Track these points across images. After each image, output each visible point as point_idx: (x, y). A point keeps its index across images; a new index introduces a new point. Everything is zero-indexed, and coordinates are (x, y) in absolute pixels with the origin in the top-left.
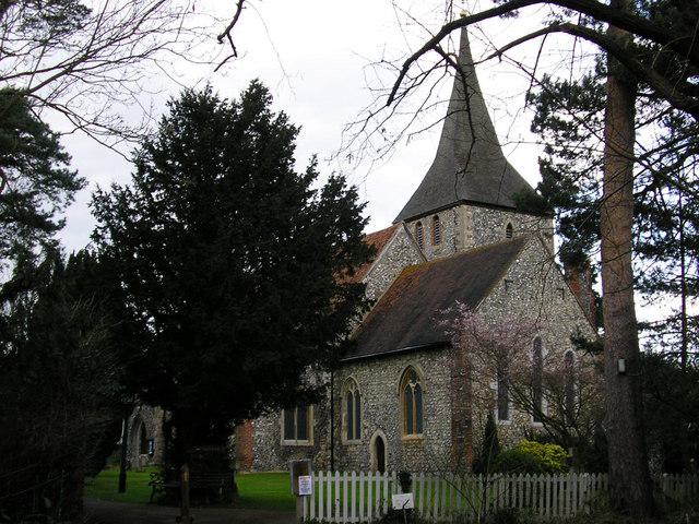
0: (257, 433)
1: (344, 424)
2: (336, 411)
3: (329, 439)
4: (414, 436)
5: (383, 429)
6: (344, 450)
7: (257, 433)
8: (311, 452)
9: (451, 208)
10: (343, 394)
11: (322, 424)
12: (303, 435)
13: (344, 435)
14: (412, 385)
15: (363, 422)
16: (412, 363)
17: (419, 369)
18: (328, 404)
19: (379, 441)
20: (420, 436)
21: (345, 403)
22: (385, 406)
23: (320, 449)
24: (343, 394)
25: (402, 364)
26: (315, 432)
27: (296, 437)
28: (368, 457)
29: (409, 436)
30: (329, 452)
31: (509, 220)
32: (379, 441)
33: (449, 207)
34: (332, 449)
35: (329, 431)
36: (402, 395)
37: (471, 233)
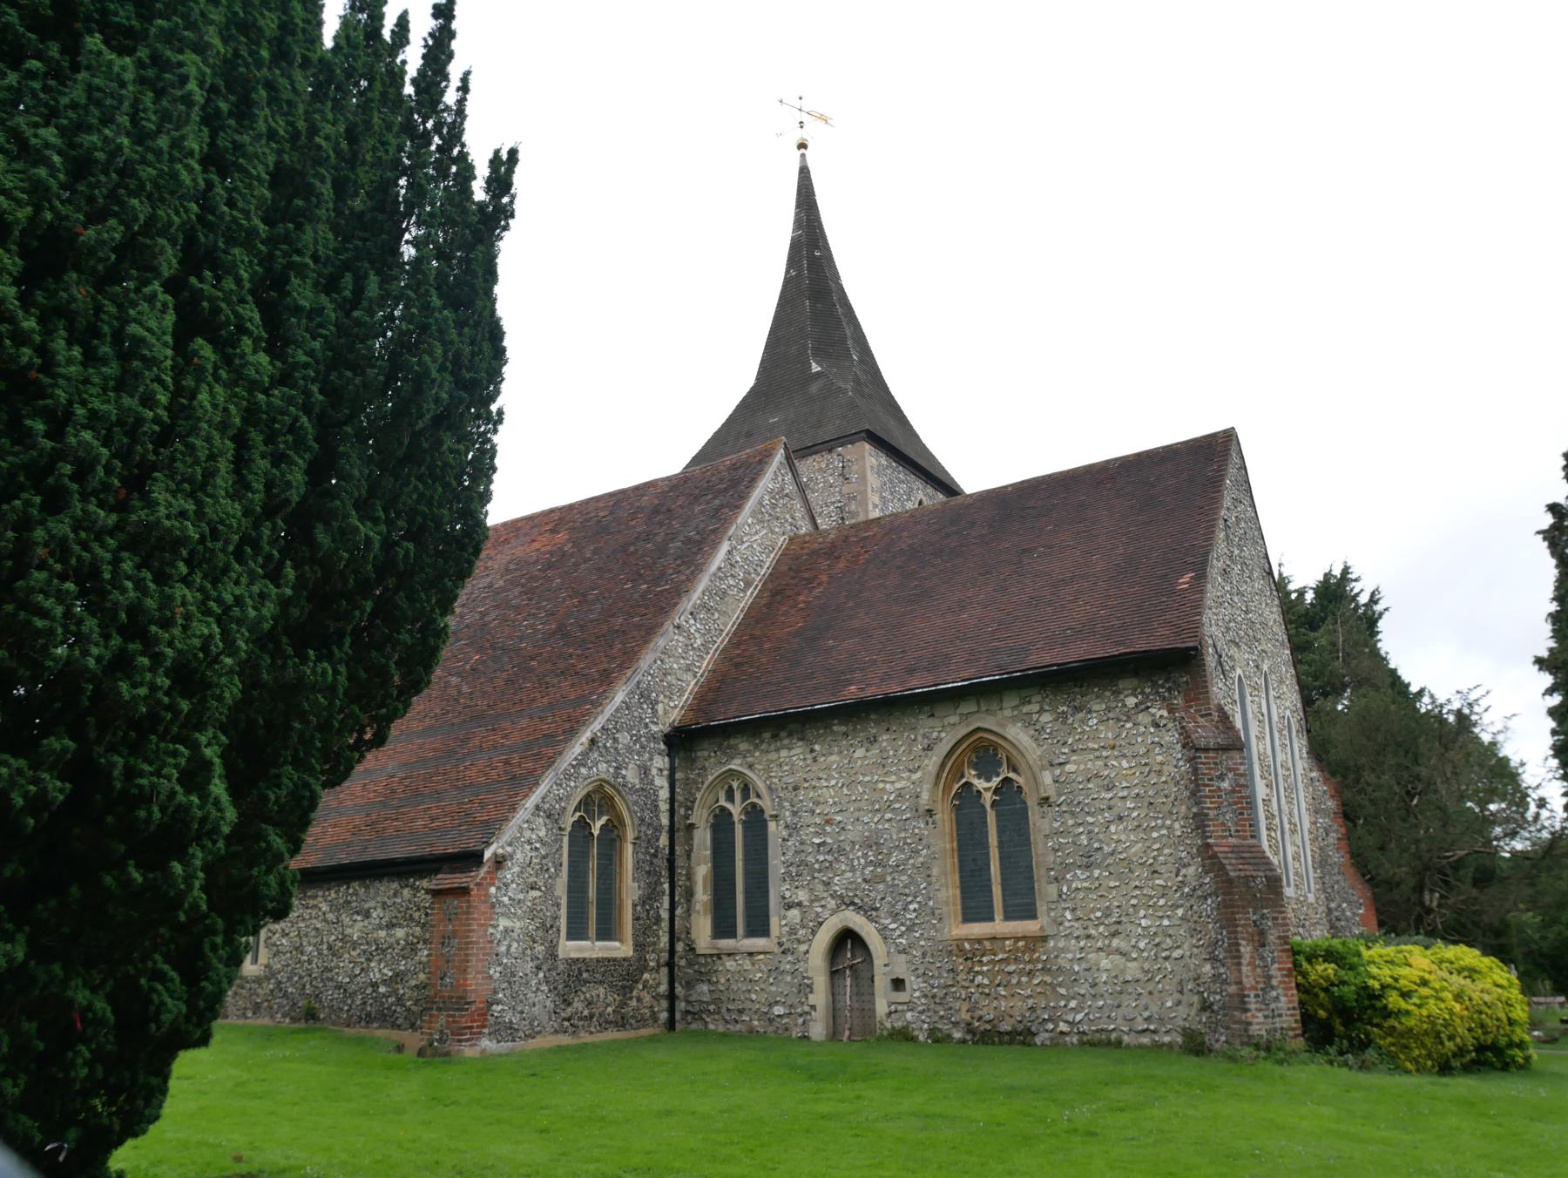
0: (503, 923)
1: (702, 896)
2: (680, 862)
3: (664, 940)
4: (999, 926)
5: (868, 911)
6: (704, 967)
7: (503, 923)
8: (624, 976)
9: (830, 451)
10: (701, 817)
11: (649, 898)
12: (607, 931)
13: (702, 929)
14: (980, 784)
15: (778, 889)
16: (988, 722)
17: (1018, 735)
18: (664, 841)
19: (847, 939)
20: (1030, 927)
21: (703, 838)
22: (871, 843)
23: (644, 968)
24: (701, 817)
25: (947, 730)
26: (636, 919)
27: (592, 931)
28: (806, 988)
29: (978, 929)
30: (665, 971)
31: (920, 495)
32: (847, 939)
33: (828, 446)
34: (671, 965)
35: (665, 915)
36: (944, 816)
37: (876, 500)
